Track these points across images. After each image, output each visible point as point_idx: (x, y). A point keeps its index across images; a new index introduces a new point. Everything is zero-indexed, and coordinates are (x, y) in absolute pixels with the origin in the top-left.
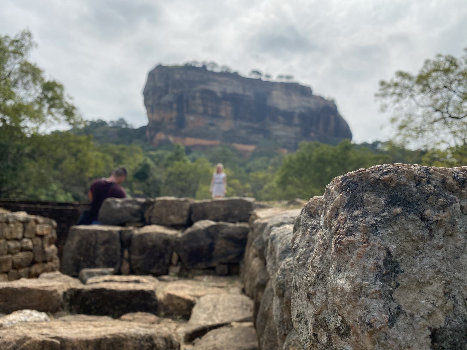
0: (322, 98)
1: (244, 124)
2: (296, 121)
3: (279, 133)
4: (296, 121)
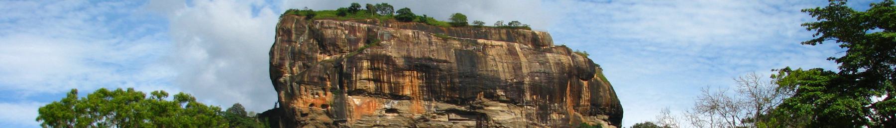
0: (568, 52)
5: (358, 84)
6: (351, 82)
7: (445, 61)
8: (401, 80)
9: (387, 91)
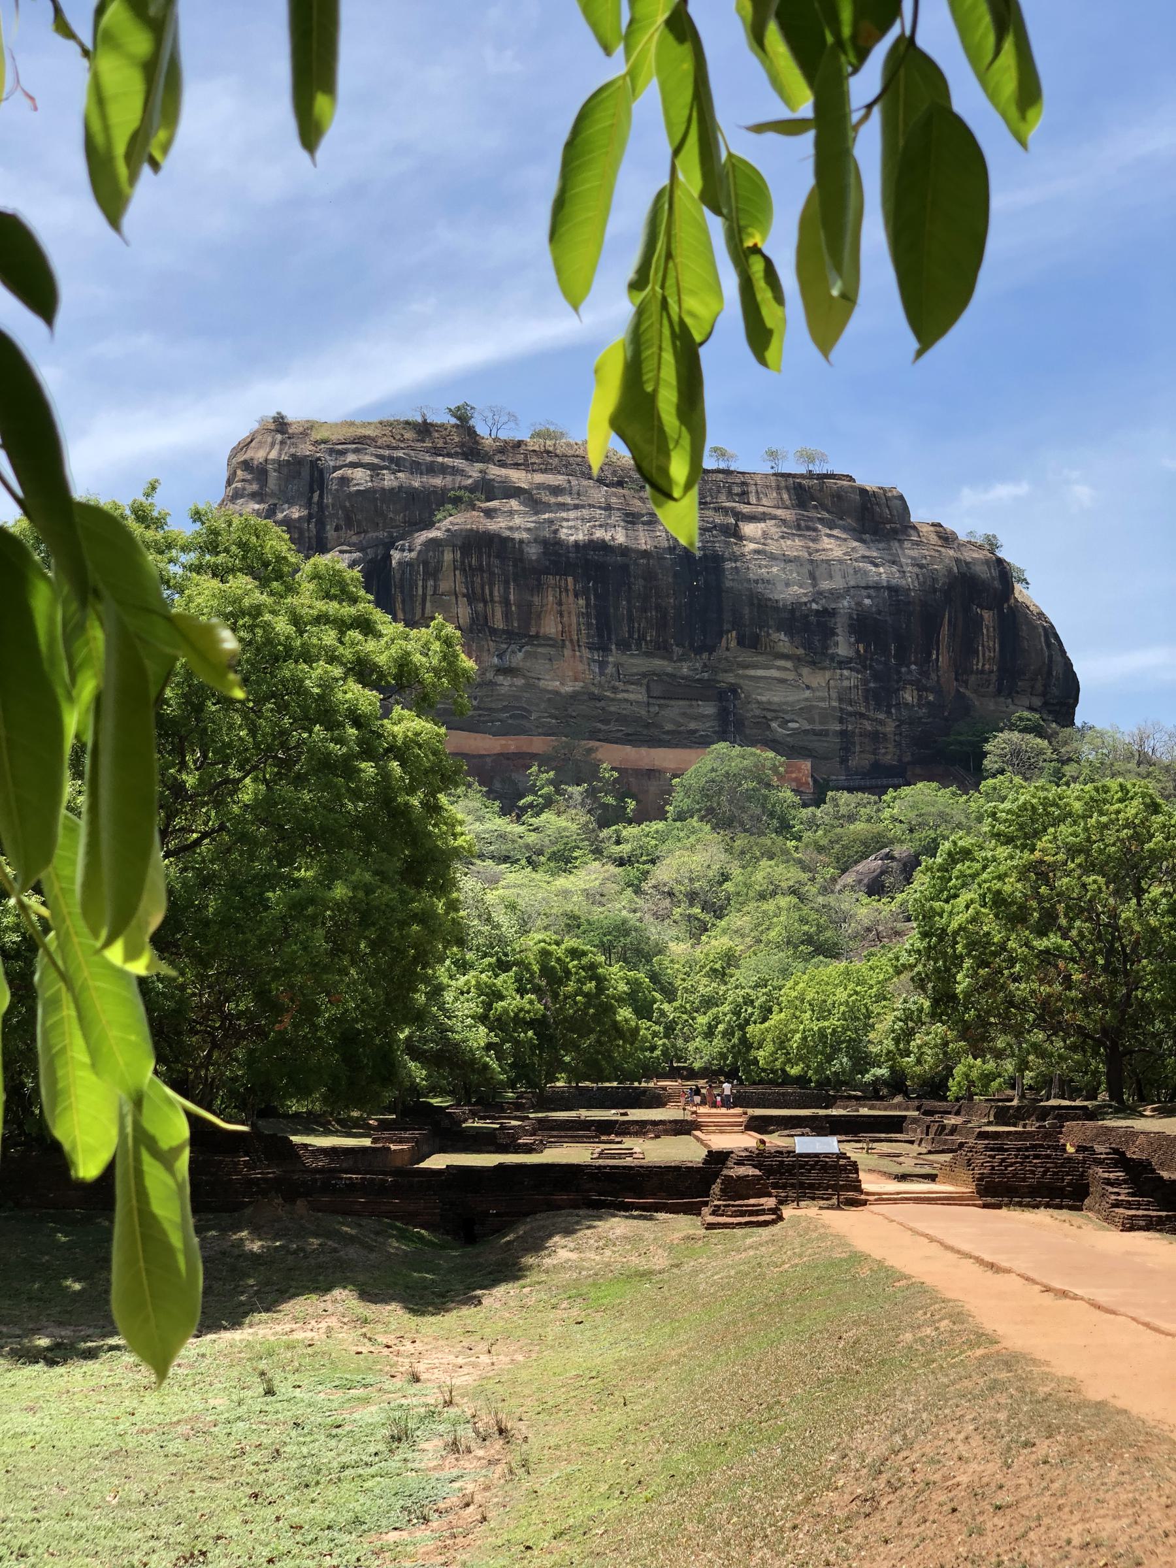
0: (947, 538)
1: (637, 663)
2: (843, 647)
3: (776, 696)
4: (843, 647)
5: (428, 604)
6: (412, 597)
7: (645, 554)
8: (536, 600)
9: (499, 624)
